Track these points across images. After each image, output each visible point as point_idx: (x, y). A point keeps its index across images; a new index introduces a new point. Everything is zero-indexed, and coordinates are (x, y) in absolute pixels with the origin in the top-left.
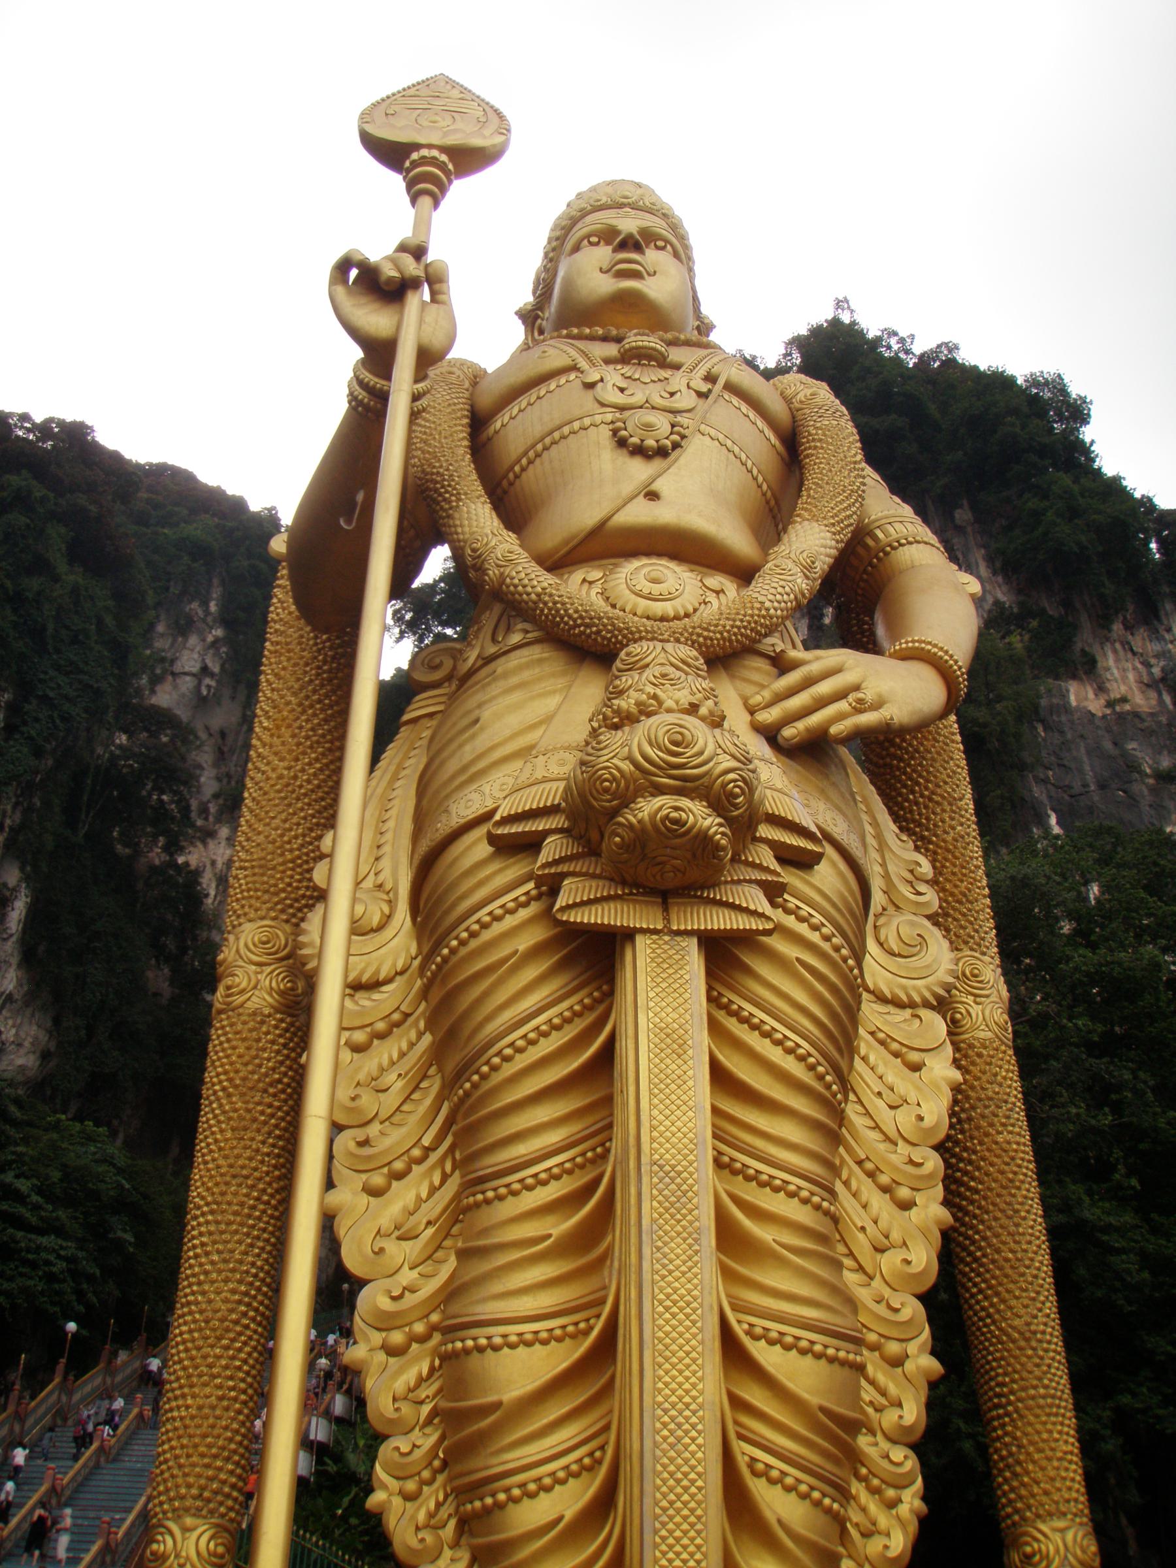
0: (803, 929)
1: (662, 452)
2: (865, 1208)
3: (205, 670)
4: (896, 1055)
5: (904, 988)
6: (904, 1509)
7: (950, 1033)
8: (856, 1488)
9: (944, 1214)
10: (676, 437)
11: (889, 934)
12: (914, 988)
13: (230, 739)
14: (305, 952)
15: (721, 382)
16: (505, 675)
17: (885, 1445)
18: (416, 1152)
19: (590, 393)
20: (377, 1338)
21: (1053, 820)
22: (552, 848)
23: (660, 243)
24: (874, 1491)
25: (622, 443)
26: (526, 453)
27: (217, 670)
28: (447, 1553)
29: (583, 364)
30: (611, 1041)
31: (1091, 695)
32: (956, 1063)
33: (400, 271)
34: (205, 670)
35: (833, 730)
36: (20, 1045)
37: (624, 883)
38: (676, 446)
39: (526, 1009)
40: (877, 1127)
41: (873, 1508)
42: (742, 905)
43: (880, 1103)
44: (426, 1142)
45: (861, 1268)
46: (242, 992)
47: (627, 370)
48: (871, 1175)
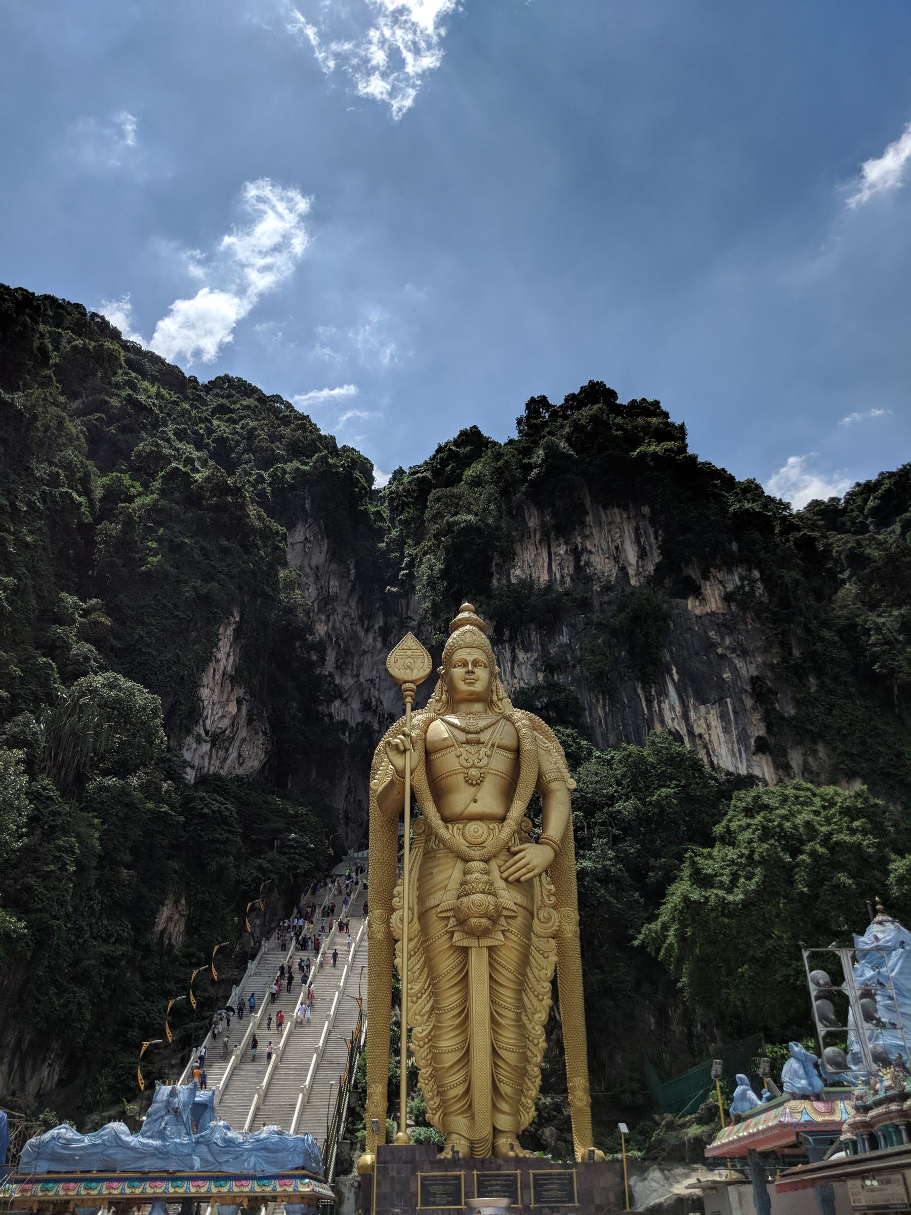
0: (513, 937)
1: (478, 784)
2: (529, 1001)
3: (306, 538)
8: (526, 1078)
11: (541, 916)
13: (321, 571)
20: (417, 1043)
21: (674, 671)
22: (452, 920)
25: (467, 781)
27: (312, 539)
30: (467, 973)
31: (697, 603)
34: (306, 538)
35: (522, 879)
37: (467, 933)
39: (447, 964)
41: (529, 1084)
42: (498, 939)
47: (468, 747)
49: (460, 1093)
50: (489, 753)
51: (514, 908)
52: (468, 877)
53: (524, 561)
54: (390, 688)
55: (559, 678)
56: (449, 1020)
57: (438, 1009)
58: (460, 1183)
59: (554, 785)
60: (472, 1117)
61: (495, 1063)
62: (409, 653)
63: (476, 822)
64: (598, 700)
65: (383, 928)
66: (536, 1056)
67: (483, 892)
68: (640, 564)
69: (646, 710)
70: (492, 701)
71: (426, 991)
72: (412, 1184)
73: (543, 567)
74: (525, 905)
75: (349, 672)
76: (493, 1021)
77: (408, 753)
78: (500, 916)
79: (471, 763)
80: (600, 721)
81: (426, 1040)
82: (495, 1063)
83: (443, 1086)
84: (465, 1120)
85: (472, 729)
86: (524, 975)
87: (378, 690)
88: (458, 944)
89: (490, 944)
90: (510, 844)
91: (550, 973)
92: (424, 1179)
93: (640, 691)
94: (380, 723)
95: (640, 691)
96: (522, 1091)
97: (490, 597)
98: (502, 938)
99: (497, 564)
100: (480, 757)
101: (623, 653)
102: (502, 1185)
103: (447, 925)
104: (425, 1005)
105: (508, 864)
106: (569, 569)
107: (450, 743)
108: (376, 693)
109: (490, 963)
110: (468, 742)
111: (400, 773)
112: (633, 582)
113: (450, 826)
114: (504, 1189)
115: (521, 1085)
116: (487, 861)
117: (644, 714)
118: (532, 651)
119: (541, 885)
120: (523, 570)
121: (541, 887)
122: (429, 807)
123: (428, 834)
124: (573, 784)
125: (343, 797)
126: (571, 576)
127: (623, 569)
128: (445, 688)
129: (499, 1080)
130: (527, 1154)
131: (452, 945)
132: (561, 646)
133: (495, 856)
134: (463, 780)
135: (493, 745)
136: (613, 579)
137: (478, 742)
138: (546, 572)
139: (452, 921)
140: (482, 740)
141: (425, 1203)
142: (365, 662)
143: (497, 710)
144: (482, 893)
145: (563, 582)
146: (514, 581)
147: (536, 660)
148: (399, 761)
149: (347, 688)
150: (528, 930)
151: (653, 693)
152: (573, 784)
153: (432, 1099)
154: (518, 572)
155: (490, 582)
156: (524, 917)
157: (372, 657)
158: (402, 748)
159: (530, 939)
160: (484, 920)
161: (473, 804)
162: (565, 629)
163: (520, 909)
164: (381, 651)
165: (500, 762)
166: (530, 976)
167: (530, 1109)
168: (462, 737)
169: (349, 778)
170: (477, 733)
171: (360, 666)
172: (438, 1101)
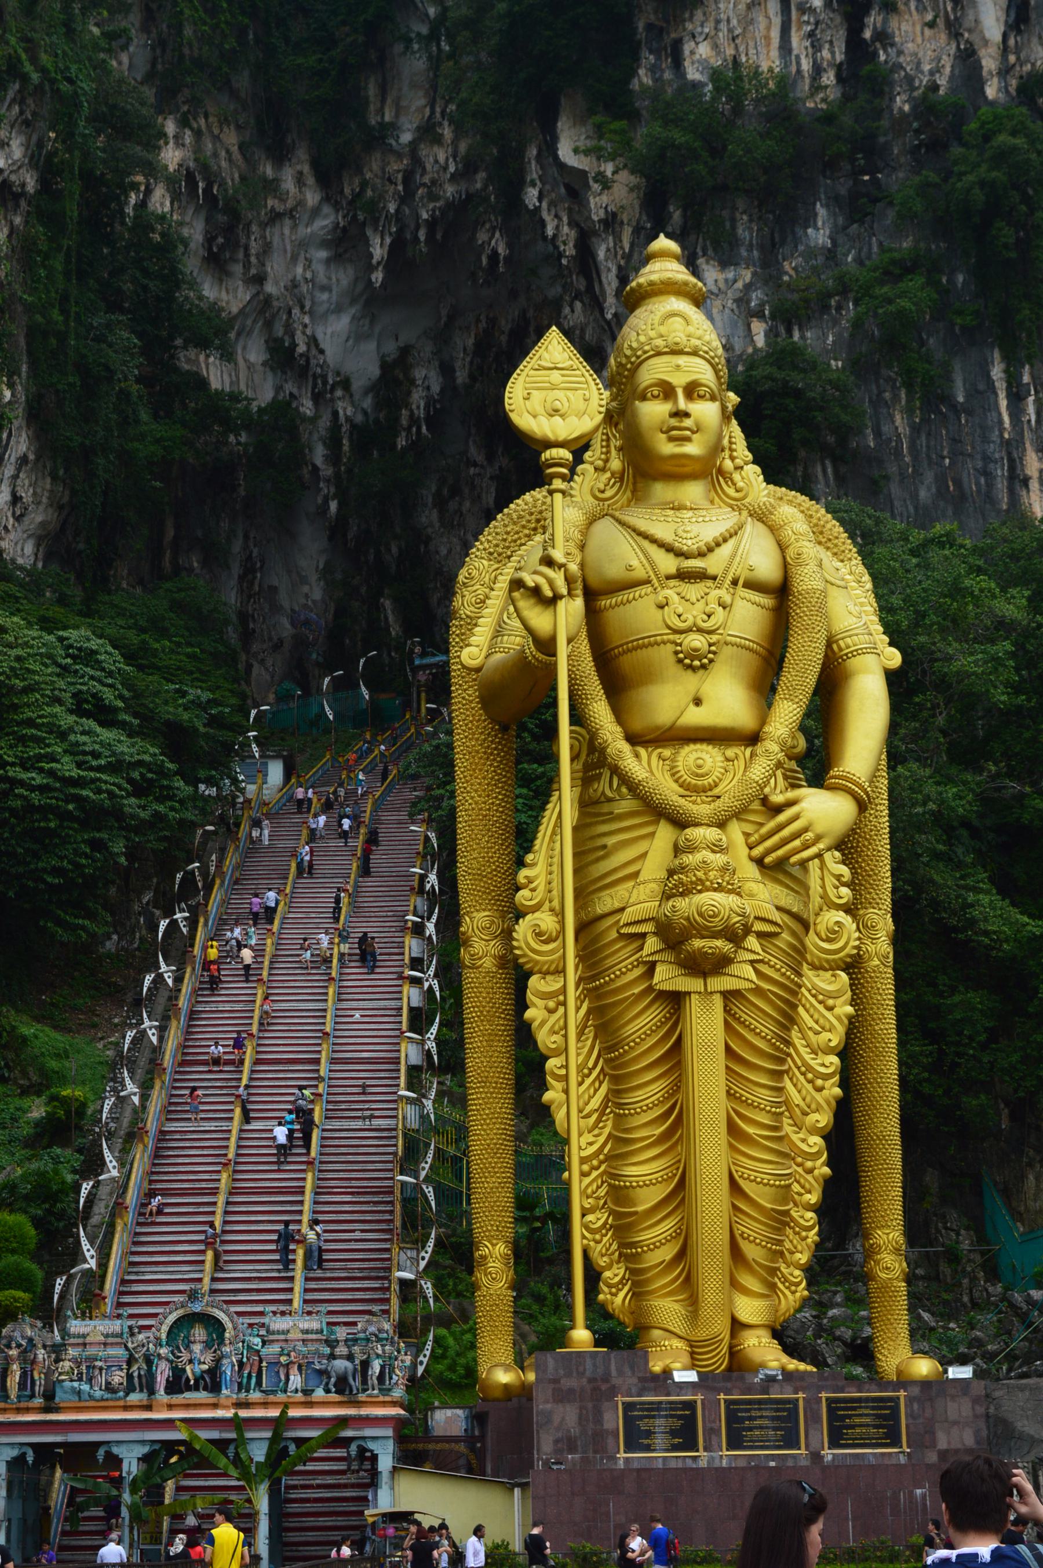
1: (703, 667)
4: (820, 1002)
5: (827, 961)
6: (809, 1240)
7: (851, 985)
9: (838, 1091)
10: (711, 656)
11: (822, 928)
12: (834, 960)
14: (517, 952)
15: (741, 582)
16: (621, 817)
17: (802, 1212)
18: (586, 1071)
19: (660, 611)
23: (702, 393)
24: (796, 1233)
26: (622, 645)
28: (615, 1266)
29: (655, 581)
32: (853, 1003)
33: (552, 589)
36: (39, 503)
38: (711, 661)
40: (808, 1046)
42: (742, 974)
43: (810, 1034)
44: (590, 1064)
45: (796, 1125)
46: (480, 959)
48: (803, 1074)
49: (668, 1258)
50: (727, 599)
51: (777, 916)
52: (688, 859)
53: (718, 22)
54: (339, 310)
55: (803, 337)
56: (645, 1126)
57: (620, 1106)
58: (693, 1416)
59: (855, 663)
60: (693, 1302)
61: (735, 1207)
62: (556, 376)
63: (698, 746)
64: (896, 398)
65: (494, 947)
66: (810, 1192)
67: (720, 889)
68: (1012, 42)
69: (1006, 419)
70: (720, 471)
71: (591, 1070)
72: (607, 1416)
73: (767, 38)
74: (795, 910)
75: (238, 269)
76: (733, 1129)
77: (561, 605)
78: (747, 930)
79: (689, 623)
80: (899, 441)
81: (595, 1163)
82: (735, 1207)
83: (633, 1245)
84: (677, 1306)
85: (689, 544)
86: (788, 1043)
87: (311, 313)
88: (667, 987)
89: (729, 987)
90: (767, 790)
91: (836, 1038)
92: (628, 1407)
93: (997, 372)
94: (317, 398)
95: (997, 372)
96: (782, 1253)
97: (633, 116)
98: (753, 976)
99: (649, 27)
100: (708, 610)
101: (960, 278)
102: (773, 1419)
103: (641, 948)
104: (591, 1097)
105: (764, 830)
106: (834, 52)
107: (640, 573)
108: (307, 320)
109: (726, 1022)
110: (683, 576)
111: (547, 645)
112: (991, 91)
113: (642, 751)
114: (776, 1424)
115: (780, 1242)
116: (722, 825)
117: (1002, 430)
118: (736, 264)
119: (823, 866)
120: (715, 47)
121: (821, 869)
122: (601, 711)
123: (594, 760)
124: (894, 658)
125: (233, 582)
126: (839, 67)
127: (968, 57)
128: (615, 443)
129: (742, 1235)
130: (802, 1366)
131: (650, 989)
132: (811, 253)
133: (738, 814)
134: (672, 659)
135: (735, 583)
136: (942, 81)
137: (702, 576)
138: (774, 53)
139: (652, 944)
140: (711, 571)
141: (631, 1446)
142: (276, 240)
143: (731, 491)
144: (715, 890)
145: (817, 87)
146: (693, 74)
147: (748, 287)
148: (540, 620)
149: (235, 310)
150: (798, 955)
151: (1026, 379)
152: (894, 658)
153: (609, 1267)
154: (704, 50)
155: (633, 73)
156: (794, 934)
157: (294, 227)
158: (549, 593)
159: (799, 975)
160: (719, 943)
161: (692, 707)
162: (821, 212)
163: (786, 918)
164: (316, 212)
165: (746, 618)
166: (798, 1042)
167: (798, 1284)
168: (668, 564)
169: (246, 537)
170: (701, 555)
171: (267, 248)
172: (622, 1271)
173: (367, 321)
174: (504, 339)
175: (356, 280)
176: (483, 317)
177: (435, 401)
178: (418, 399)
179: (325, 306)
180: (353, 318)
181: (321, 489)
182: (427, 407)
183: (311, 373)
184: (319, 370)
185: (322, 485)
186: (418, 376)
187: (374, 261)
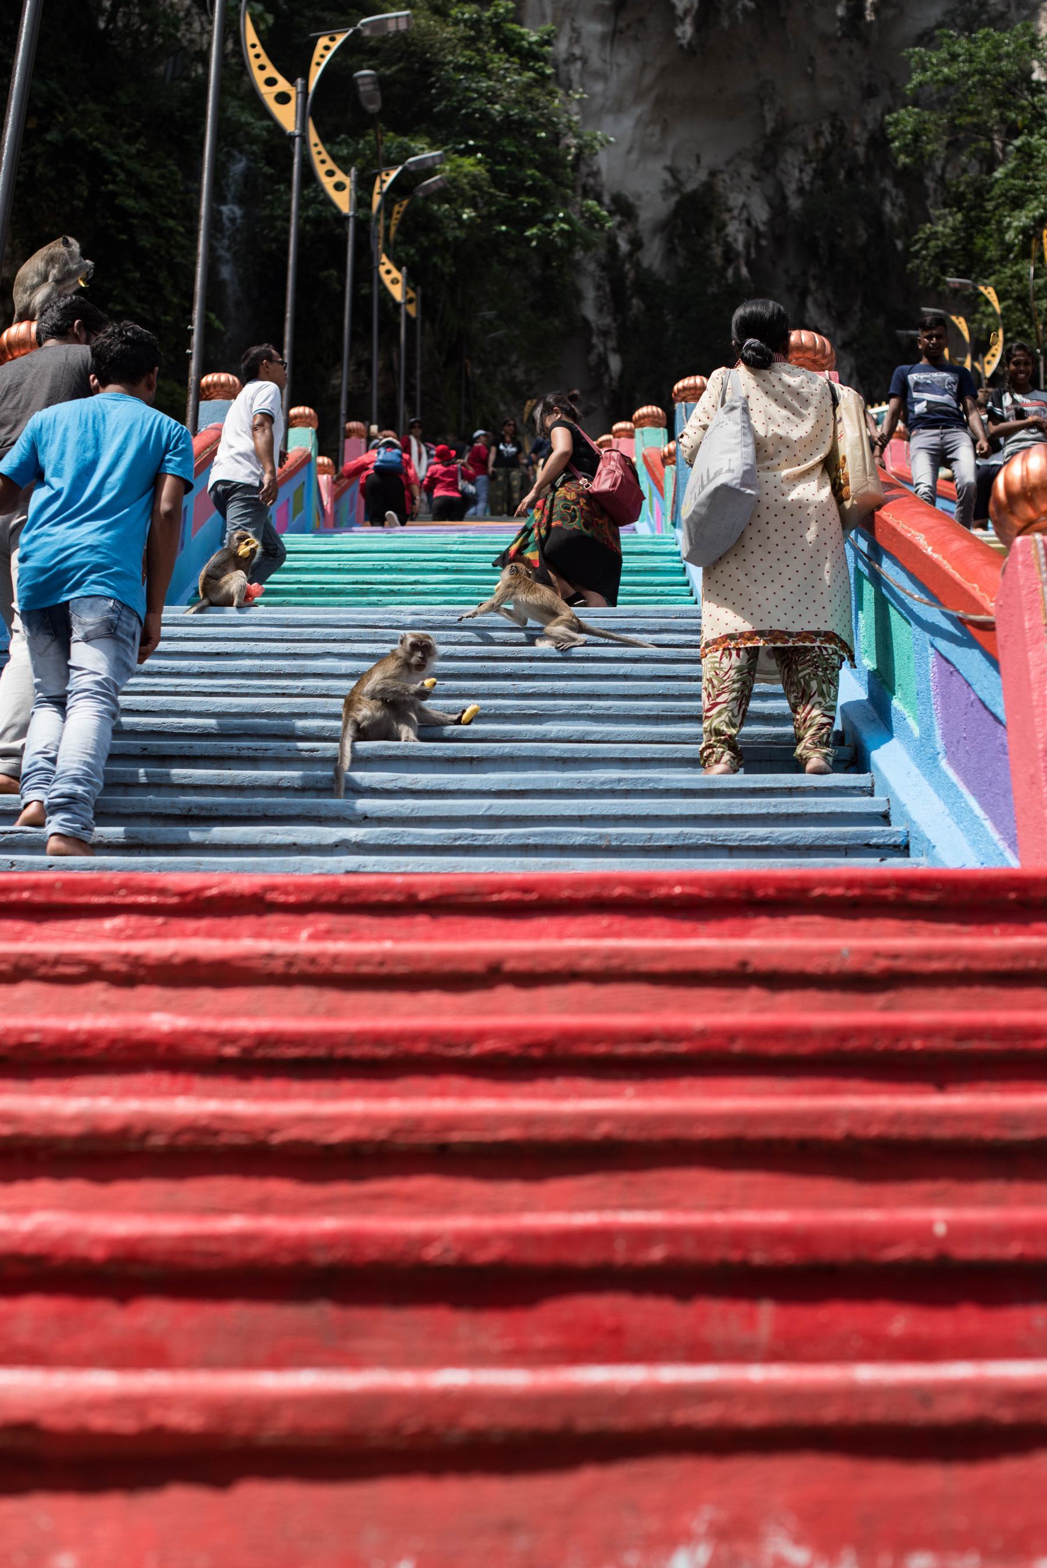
54: (618, 108)
173: (657, 129)
174: (860, 151)
175: (645, 65)
176: (826, 127)
177: (758, 234)
178: (736, 233)
179: (599, 100)
180: (638, 121)
181: (590, 348)
182: (747, 245)
183: (579, 183)
184: (591, 181)
185: (595, 340)
186: (731, 203)
187: (680, 11)
